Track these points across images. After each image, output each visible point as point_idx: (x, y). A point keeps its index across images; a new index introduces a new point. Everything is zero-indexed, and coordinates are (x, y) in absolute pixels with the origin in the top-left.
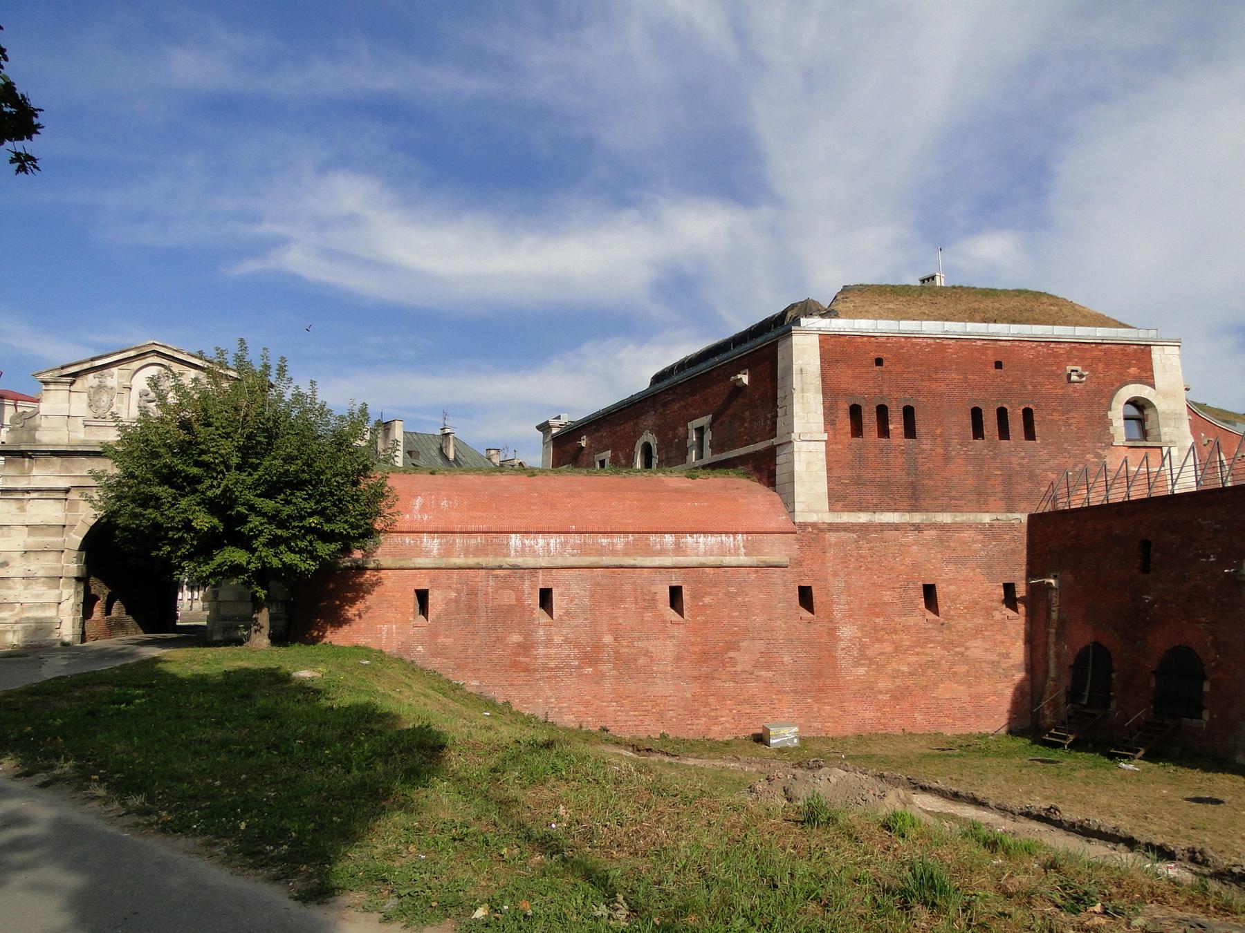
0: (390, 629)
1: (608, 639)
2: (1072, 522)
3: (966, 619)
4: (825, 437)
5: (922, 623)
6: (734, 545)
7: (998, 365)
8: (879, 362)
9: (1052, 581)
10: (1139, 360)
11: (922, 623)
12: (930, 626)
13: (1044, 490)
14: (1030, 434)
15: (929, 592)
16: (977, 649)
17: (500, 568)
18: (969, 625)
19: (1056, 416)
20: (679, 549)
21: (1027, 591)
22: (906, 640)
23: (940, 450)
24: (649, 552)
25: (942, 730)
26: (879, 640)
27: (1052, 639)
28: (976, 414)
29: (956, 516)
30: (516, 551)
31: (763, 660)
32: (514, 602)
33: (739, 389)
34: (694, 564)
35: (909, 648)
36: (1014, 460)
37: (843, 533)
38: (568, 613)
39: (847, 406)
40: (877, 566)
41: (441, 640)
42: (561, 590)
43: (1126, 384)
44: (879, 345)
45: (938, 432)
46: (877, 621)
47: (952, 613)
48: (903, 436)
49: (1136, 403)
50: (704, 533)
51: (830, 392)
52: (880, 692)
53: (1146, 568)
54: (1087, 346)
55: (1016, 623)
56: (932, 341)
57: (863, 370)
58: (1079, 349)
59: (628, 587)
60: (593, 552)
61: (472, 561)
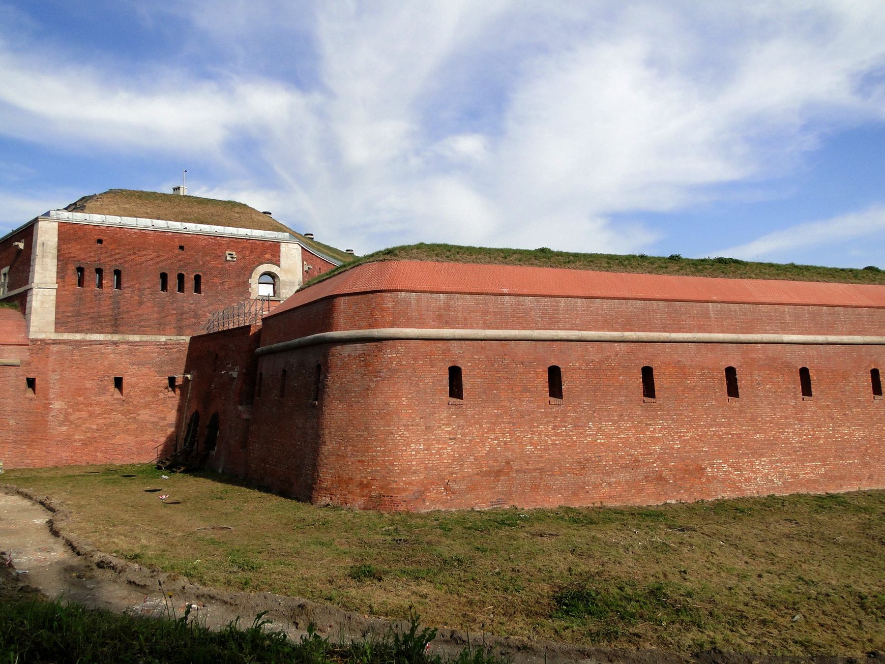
3: (140, 397)
4: (56, 286)
5: (110, 400)
7: (182, 248)
8: (100, 241)
10: (272, 250)
12: (115, 402)
14: (198, 289)
16: (145, 415)
18: (142, 401)
19: (216, 280)
23: (136, 297)
25: (115, 462)
26: (79, 410)
28: (164, 276)
35: (99, 415)
36: (185, 304)
37: (63, 346)
39: (74, 268)
43: (263, 264)
44: (102, 231)
45: (137, 286)
51: (63, 259)
52: (75, 441)
54: (240, 240)
55: (173, 398)
56: (136, 231)
57: (88, 246)
58: (235, 241)
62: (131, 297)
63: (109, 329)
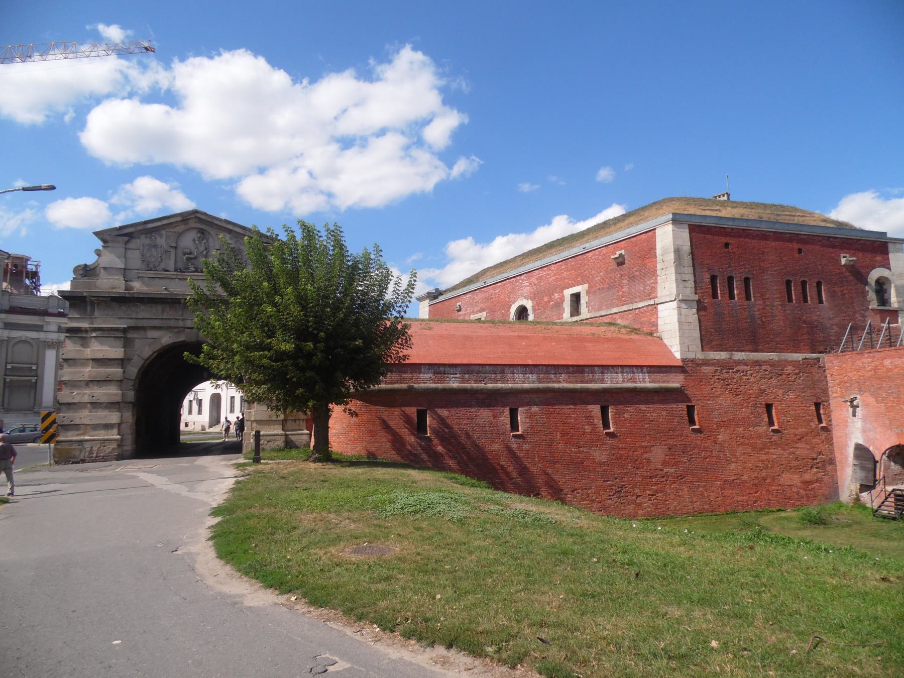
28: (788, 283)
62: (764, 309)
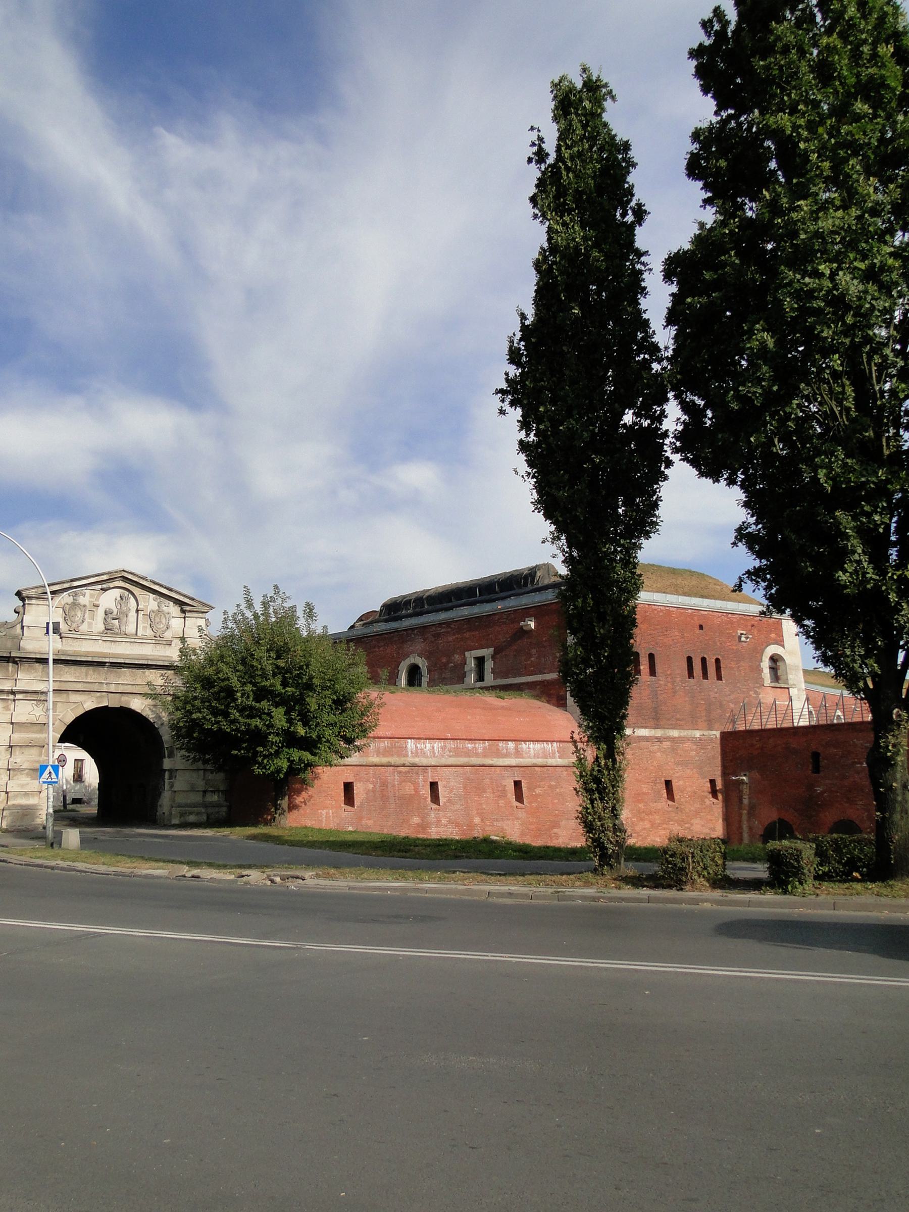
0: (327, 813)
1: (477, 820)
2: (757, 738)
6: (552, 750)
9: (744, 778)
10: (775, 628)
11: (666, 807)
13: (728, 715)
14: (719, 678)
15: (668, 783)
17: (404, 765)
18: (692, 808)
19: (733, 665)
20: (518, 753)
21: (722, 785)
22: (657, 819)
23: (670, 685)
24: (499, 754)
26: (642, 820)
27: (745, 817)
29: (680, 732)
30: (412, 753)
31: (574, 834)
32: (413, 792)
33: (524, 633)
34: (530, 764)
36: (712, 694)
38: (449, 801)
40: (637, 767)
41: (364, 822)
42: (444, 783)
45: (668, 673)
46: (640, 806)
47: (682, 800)
48: (649, 674)
49: (774, 659)
50: (533, 741)
53: (817, 769)
54: (748, 618)
55: (717, 807)
56: (662, 608)
59: (487, 781)
60: (462, 754)
61: (384, 760)
63: (651, 723)
